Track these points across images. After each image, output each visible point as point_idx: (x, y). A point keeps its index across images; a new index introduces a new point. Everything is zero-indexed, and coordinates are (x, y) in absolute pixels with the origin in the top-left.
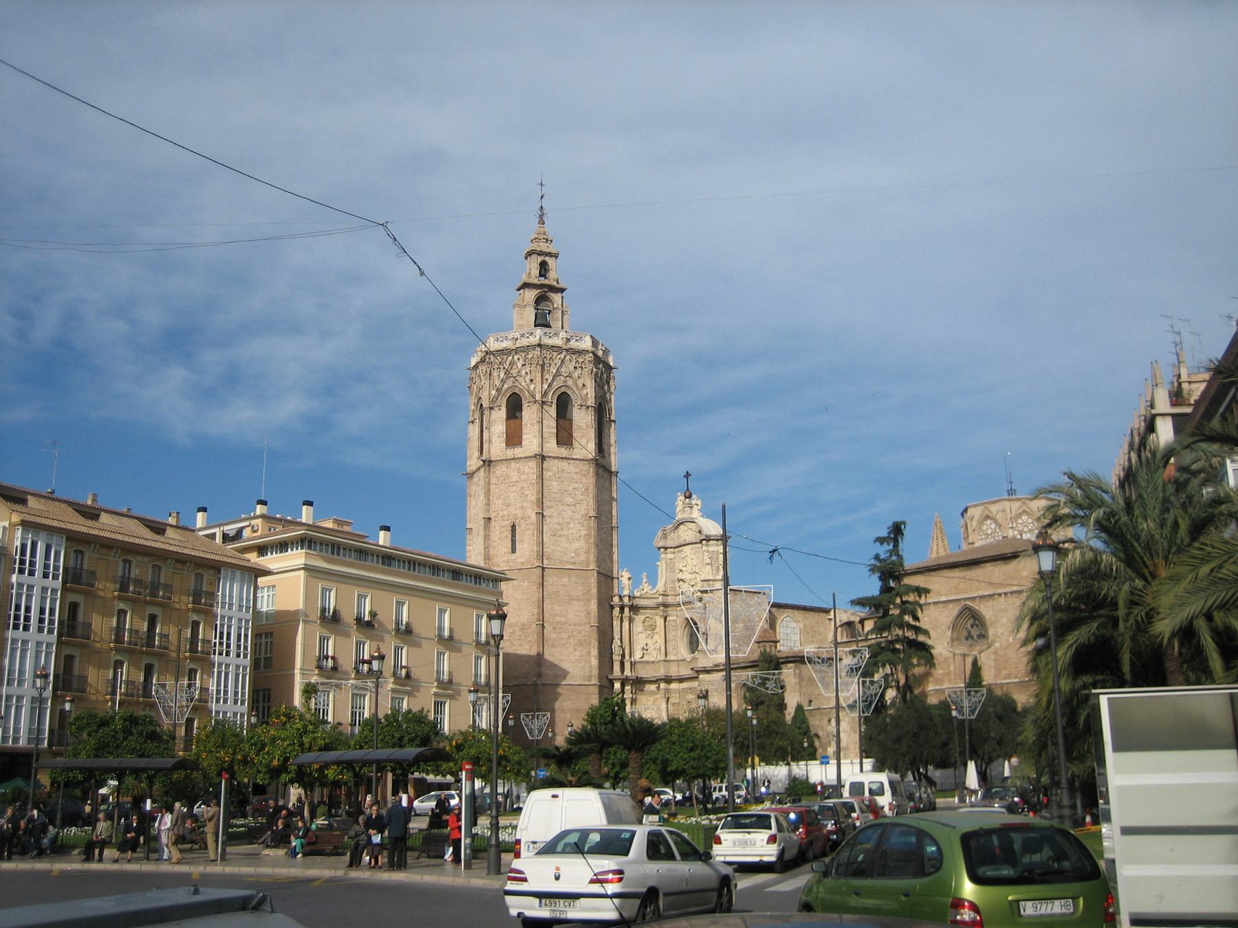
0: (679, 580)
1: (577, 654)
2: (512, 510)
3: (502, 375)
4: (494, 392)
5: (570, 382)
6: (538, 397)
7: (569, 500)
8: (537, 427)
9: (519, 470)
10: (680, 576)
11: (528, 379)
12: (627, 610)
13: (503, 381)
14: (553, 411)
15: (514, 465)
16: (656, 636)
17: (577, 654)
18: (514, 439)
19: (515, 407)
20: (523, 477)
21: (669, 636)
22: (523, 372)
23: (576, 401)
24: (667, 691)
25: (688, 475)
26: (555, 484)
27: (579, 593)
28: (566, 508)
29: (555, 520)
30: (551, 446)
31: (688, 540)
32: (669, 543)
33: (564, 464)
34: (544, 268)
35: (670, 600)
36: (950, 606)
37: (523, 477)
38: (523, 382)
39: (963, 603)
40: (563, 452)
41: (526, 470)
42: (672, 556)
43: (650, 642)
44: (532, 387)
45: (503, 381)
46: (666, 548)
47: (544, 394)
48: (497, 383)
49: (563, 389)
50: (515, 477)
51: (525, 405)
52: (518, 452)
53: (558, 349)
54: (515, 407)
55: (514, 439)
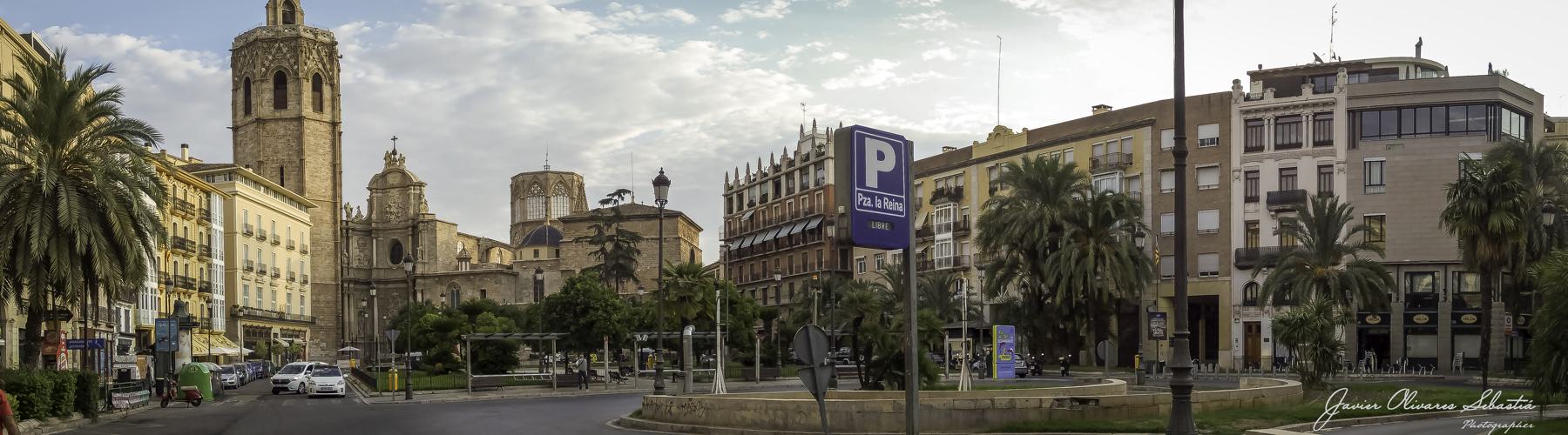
2: (280, 156)
18: (280, 102)
19: (281, 81)
30: (308, 110)
38: (286, 65)
40: (317, 116)
50: (282, 132)
52: (283, 114)
54: (281, 81)
55: (280, 102)
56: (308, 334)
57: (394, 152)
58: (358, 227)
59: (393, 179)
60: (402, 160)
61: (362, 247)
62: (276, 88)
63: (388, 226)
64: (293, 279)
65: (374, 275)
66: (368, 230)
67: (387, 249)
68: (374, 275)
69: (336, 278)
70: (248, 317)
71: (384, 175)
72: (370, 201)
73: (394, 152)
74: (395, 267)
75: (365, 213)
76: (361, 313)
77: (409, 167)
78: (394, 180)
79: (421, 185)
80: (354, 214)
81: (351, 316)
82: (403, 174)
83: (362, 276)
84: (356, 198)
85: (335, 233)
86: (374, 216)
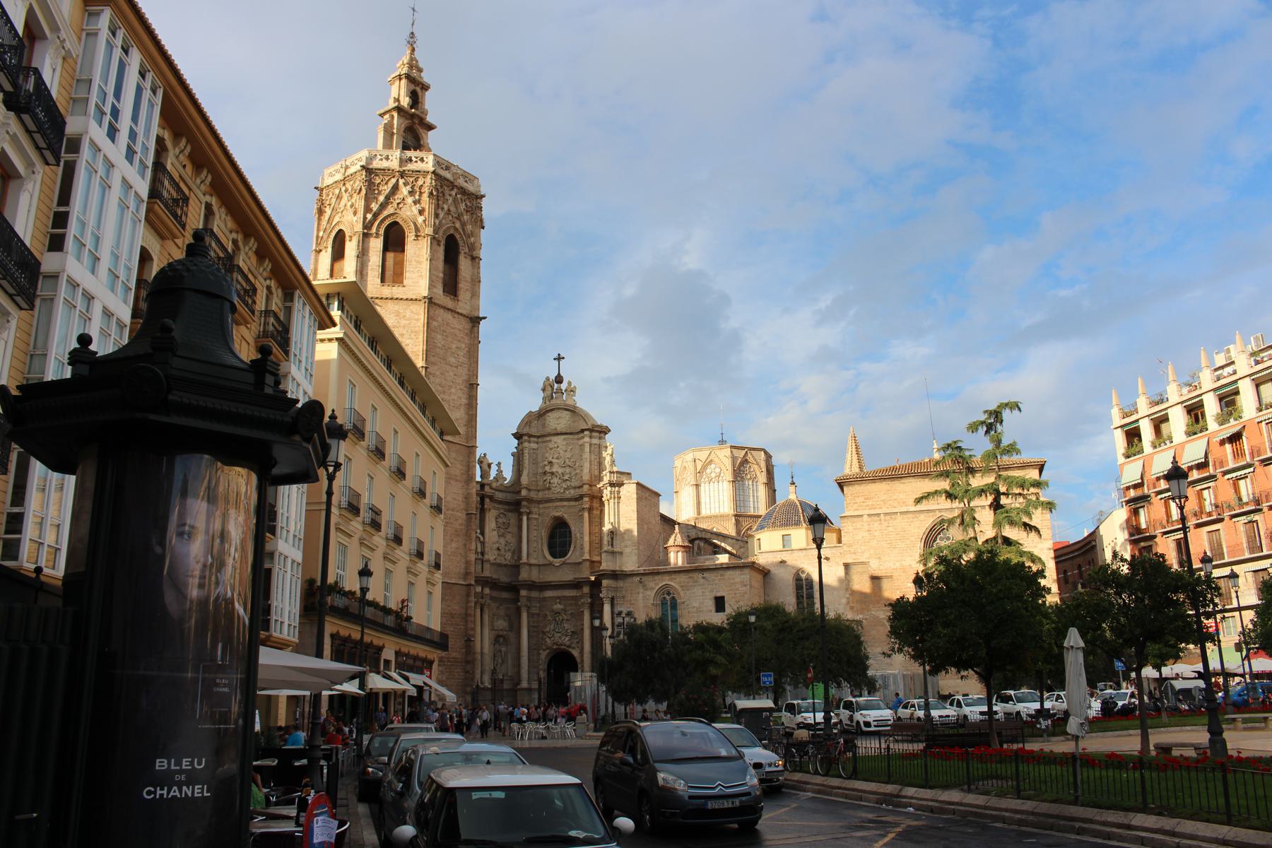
0: (545, 473)
1: (454, 545)
3: (382, 198)
4: (369, 216)
5: (458, 225)
6: (429, 231)
7: (452, 360)
8: (426, 266)
9: (397, 314)
10: (547, 468)
11: (415, 209)
12: (487, 500)
13: (383, 206)
14: (441, 250)
15: (390, 305)
16: (509, 536)
17: (454, 545)
20: (403, 322)
21: (531, 537)
22: (410, 200)
23: (463, 250)
24: (529, 599)
25: (559, 358)
26: (439, 337)
27: (458, 472)
28: (448, 367)
29: (438, 381)
31: (559, 429)
32: (534, 431)
33: (449, 316)
34: (415, 98)
35: (533, 495)
36: (922, 516)
37: (403, 322)
39: (938, 514)
40: (447, 301)
41: (408, 314)
42: (534, 446)
43: (502, 541)
44: (420, 219)
45: (383, 206)
46: (531, 436)
47: (436, 231)
48: (375, 207)
49: (452, 232)
51: (410, 237)
52: (397, 291)
53: (452, 185)
54: (394, 240)
56: (435, 666)
57: (559, 379)
58: (499, 496)
59: (558, 421)
60: (572, 391)
61: (502, 528)
62: (386, 249)
63: (548, 495)
64: (420, 555)
65: (524, 575)
66: (513, 501)
67: (544, 534)
68: (524, 575)
69: (467, 574)
70: (344, 614)
71: (541, 414)
72: (518, 457)
73: (559, 379)
74: (557, 562)
75: (508, 474)
76: (498, 639)
77: (582, 402)
78: (556, 422)
79: (603, 431)
80: (493, 473)
81: (484, 642)
82: (573, 411)
83: (504, 578)
84: (496, 446)
85: (467, 498)
86: (525, 480)
